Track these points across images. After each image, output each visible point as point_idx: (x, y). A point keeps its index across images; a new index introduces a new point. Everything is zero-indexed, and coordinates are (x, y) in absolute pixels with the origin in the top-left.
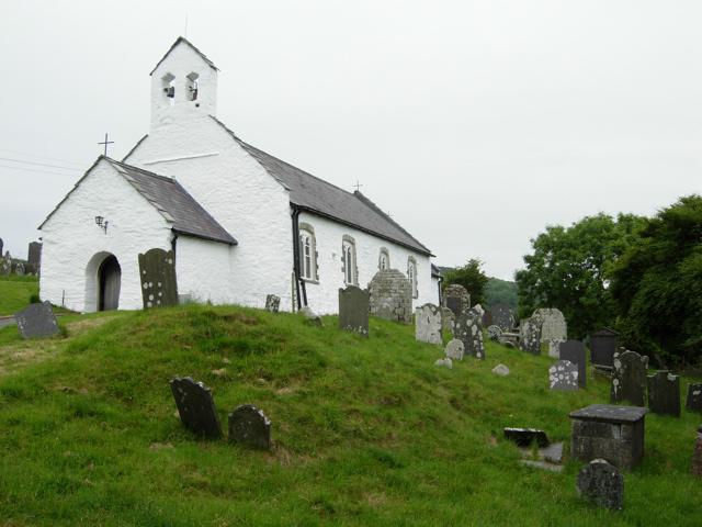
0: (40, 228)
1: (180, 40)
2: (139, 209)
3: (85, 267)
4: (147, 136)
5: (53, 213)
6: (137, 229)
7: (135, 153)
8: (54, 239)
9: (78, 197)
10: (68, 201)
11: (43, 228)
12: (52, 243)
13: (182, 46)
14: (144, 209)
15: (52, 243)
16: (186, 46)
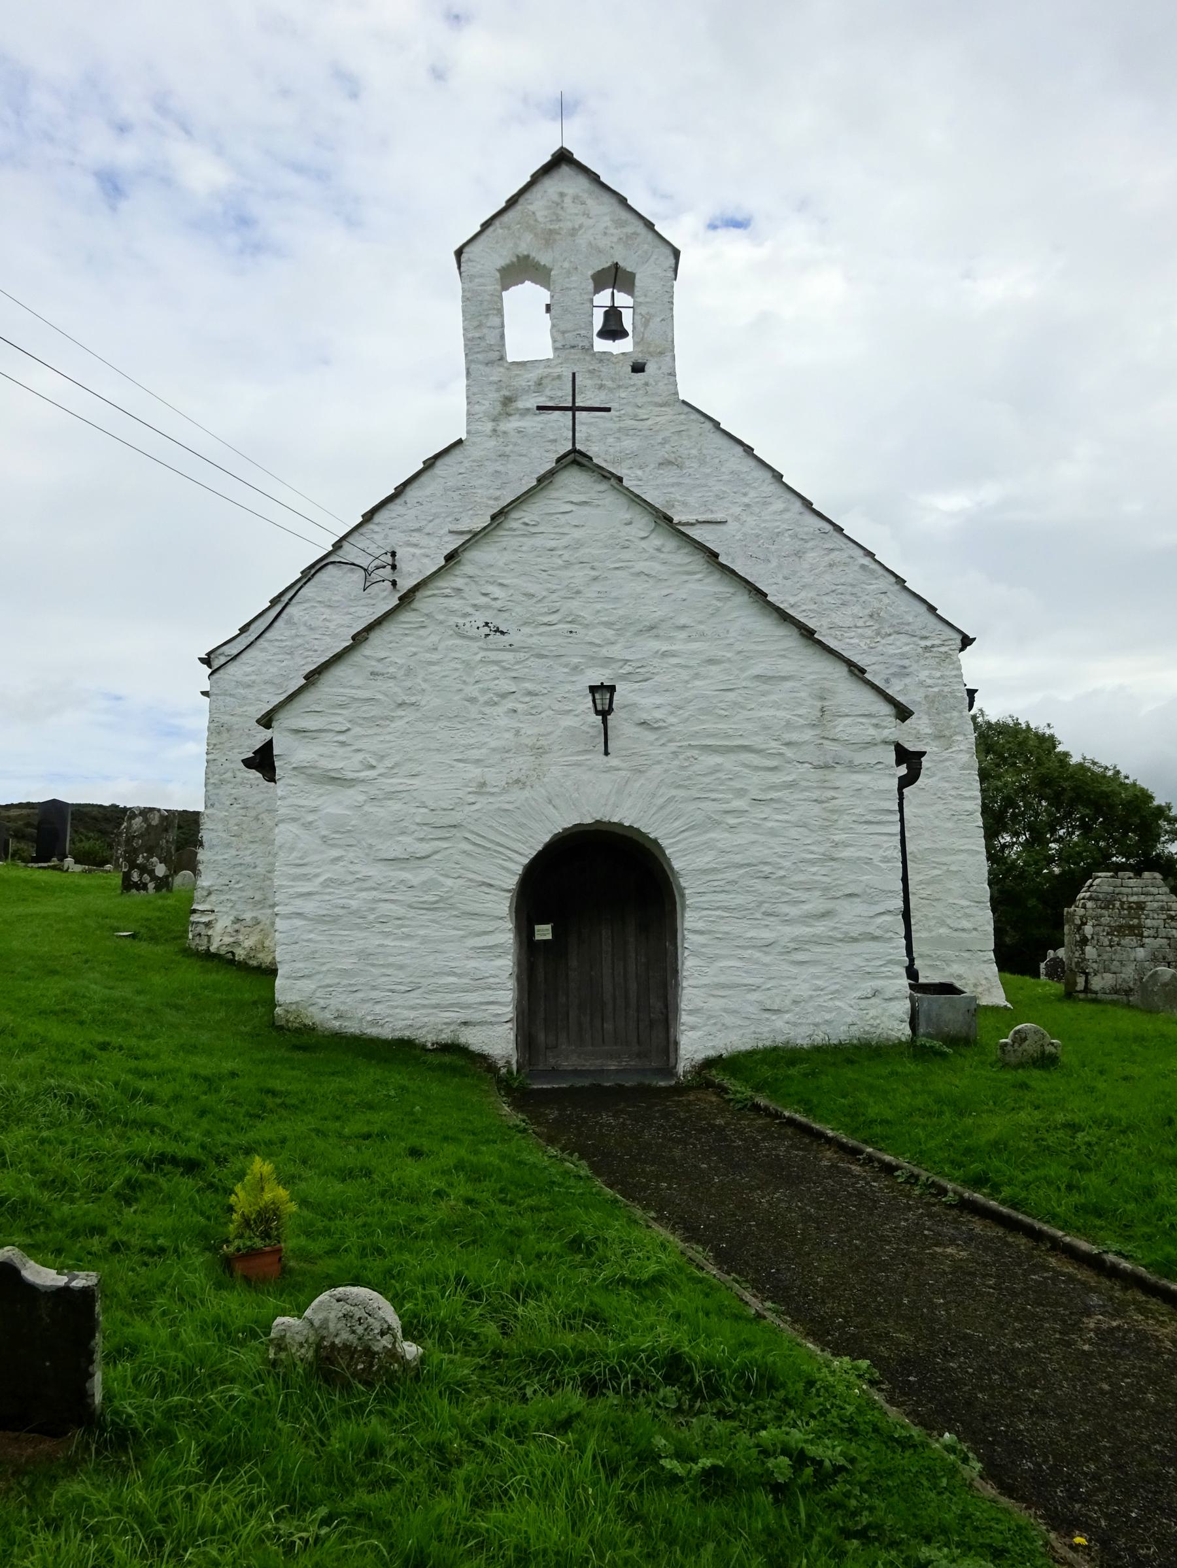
0: (267, 721)
1: (562, 158)
2: (760, 667)
3: (512, 882)
4: (460, 442)
5: (337, 658)
6: (756, 741)
7: (412, 494)
8: (346, 763)
9: (455, 603)
10: (407, 617)
11: (285, 720)
12: (335, 780)
13: (565, 183)
14: (786, 667)
15: (335, 780)
16: (583, 182)
